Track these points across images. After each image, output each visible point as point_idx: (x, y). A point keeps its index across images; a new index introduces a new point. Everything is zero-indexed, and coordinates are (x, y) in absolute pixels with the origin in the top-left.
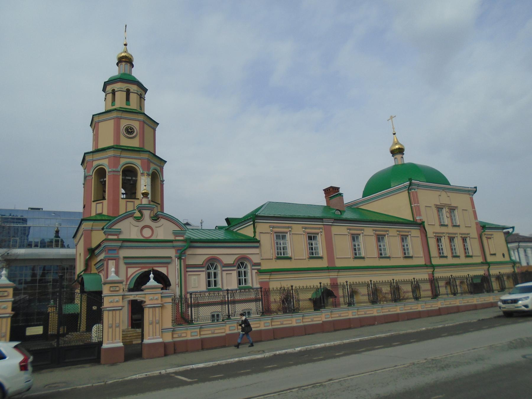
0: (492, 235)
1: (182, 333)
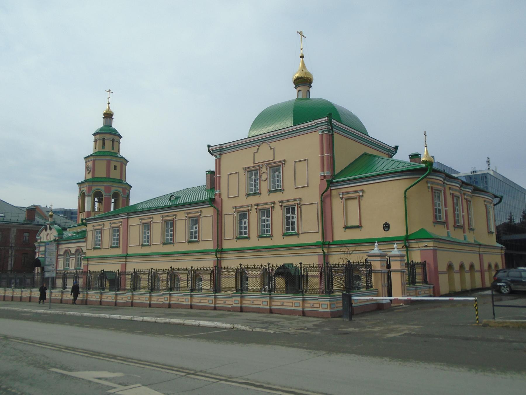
0: (357, 192)
1: (202, 299)
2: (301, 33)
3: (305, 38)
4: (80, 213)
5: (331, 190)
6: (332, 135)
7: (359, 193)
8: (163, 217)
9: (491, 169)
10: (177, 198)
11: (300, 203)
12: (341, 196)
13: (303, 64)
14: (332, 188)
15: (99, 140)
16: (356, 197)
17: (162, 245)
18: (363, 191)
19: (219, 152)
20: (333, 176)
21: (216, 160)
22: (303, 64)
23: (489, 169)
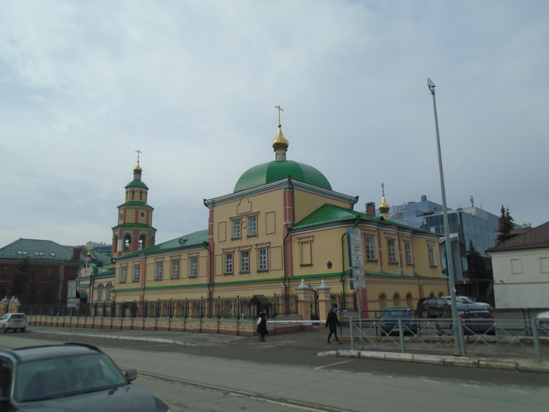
0: (309, 237)
2: (279, 107)
3: (283, 110)
4: (114, 252)
5: (291, 236)
6: (293, 192)
7: (310, 238)
8: (171, 257)
9: (474, 206)
10: (185, 241)
11: (269, 246)
12: (298, 241)
13: (281, 132)
14: (292, 234)
15: (129, 192)
16: (308, 241)
17: (170, 280)
18: (313, 237)
19: (212, 205)
20: (294, 225)
21: (210, 211)
22: (281, 132)
23: (473, 206)
